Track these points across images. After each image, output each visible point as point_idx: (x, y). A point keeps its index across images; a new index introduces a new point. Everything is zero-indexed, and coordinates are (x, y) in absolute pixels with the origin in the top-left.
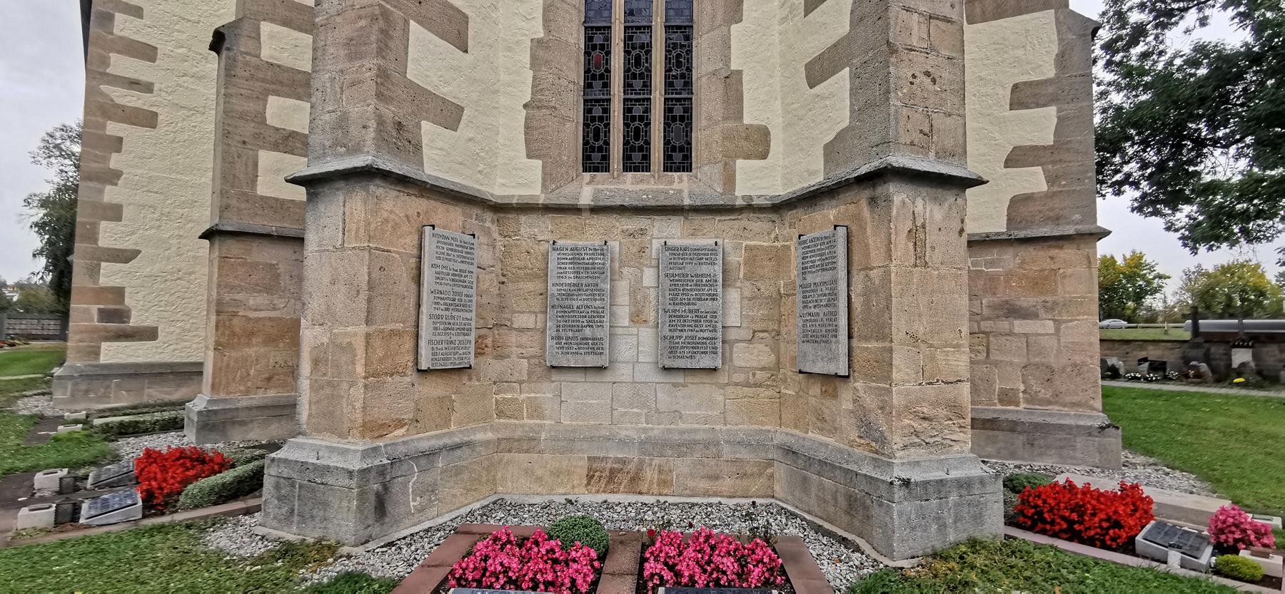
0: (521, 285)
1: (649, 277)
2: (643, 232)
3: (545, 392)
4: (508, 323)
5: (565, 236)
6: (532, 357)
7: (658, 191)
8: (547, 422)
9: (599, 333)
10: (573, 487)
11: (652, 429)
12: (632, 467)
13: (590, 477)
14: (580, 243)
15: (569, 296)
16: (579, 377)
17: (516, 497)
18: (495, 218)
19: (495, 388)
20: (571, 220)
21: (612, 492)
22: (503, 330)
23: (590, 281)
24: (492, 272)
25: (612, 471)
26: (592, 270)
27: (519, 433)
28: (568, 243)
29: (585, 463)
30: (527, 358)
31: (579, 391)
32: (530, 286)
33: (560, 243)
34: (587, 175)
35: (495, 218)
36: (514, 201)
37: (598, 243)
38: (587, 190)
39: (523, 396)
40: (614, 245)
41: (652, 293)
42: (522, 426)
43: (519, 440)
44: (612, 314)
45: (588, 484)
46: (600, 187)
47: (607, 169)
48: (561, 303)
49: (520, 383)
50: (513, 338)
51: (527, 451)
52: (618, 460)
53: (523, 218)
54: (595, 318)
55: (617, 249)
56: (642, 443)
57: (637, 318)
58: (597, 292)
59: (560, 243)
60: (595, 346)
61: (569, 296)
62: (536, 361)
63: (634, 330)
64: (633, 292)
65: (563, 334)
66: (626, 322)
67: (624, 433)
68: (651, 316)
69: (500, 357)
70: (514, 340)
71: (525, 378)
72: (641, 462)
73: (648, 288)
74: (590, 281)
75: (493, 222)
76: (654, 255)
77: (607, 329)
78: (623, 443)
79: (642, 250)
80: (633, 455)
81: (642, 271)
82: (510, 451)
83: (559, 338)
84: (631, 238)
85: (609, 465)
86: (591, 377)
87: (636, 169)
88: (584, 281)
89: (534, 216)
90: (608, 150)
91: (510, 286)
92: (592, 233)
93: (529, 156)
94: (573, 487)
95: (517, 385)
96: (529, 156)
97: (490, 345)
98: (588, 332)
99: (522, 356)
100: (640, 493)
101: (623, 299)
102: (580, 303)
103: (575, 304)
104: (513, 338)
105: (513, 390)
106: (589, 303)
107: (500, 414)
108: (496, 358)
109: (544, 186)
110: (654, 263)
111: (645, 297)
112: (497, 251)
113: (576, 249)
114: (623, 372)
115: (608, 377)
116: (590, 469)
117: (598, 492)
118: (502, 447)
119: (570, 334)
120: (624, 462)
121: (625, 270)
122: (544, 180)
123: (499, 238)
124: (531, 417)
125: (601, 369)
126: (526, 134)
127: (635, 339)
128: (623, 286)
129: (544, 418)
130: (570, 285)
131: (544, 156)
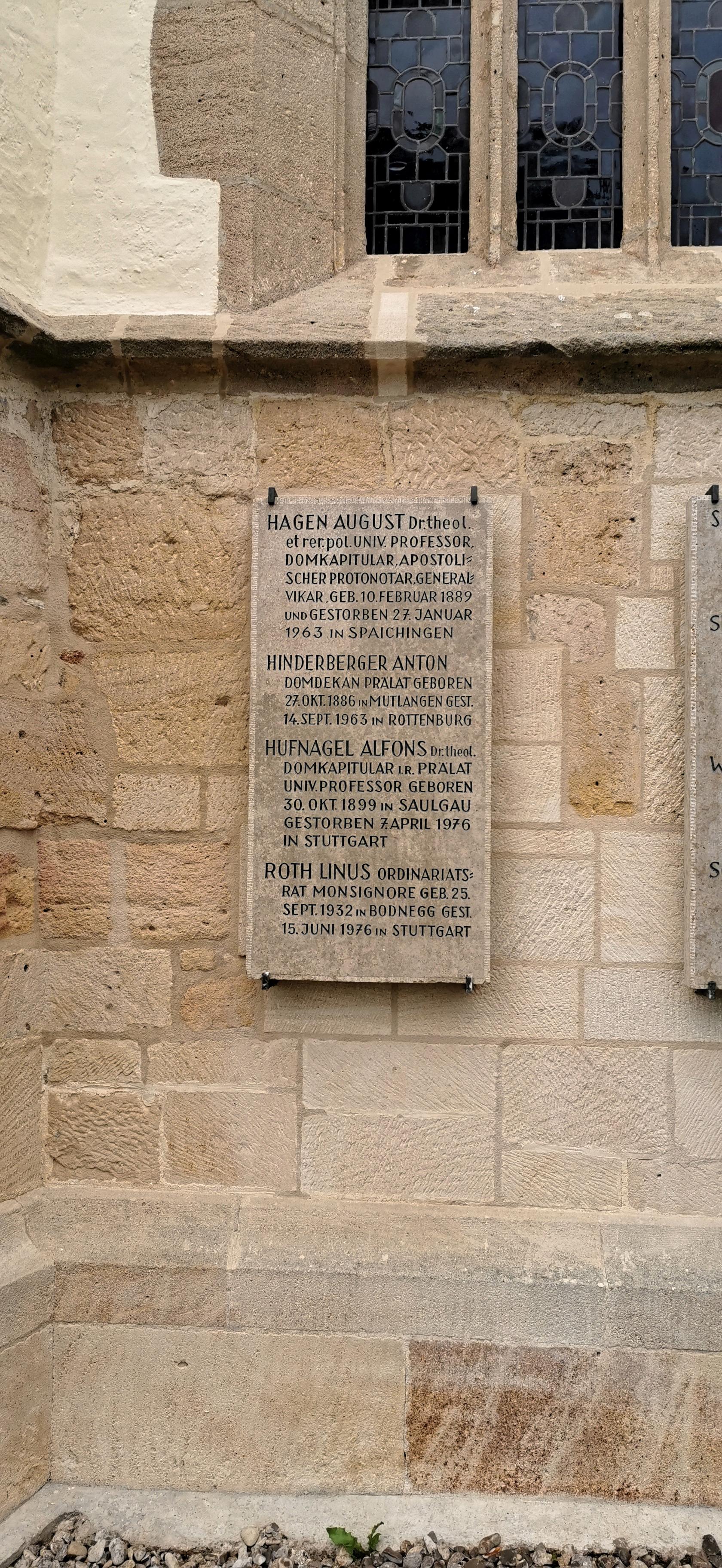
0: (145, 664)
1: (641, 635)
2: (614, 458)
3: (242, 1076)
4: (98, 812)
5: (313, 478)
6: (190, 940)
7: (668, 298)
8: (249, 1195)
9: (449, 849)
10: (355, 1466)
11: (661, 1230)
12: (590, 1389)
13: (422, 1427)
14: (376, 503)
15: (334, 704)
16: (371, 1020)
17: (127, 1505)
18: (44, 406)
19: (48, 1057)
20: (330, 417)
21: (512, 1487)
22: (74, 838)
23: (415, 646)
24: (34, 615)
25: (510, 1405)
26: (415, 600)
27: (136, 1243)
28: (328, 500)
29: (400, 1371)
30: (173, 945)
31: (378, 1088)
32: (180, 668)
33: (291, 502)
34: (386, 264)
35: (44, 406)
36: (117, 333)
37: (444, 500)
38: (394, 304)
39: (156, 1090)
40: (505, 509)
41: (656, 700)
42: (152, 1209)
43: (139, 1272)
44: (499, 780)
45: (415, 1452)
46: (442, 291)
47: (458, 242)
48: (302, 732)
49: (143, 1036)
50: (114, 870)
51: (173, 1318)
52: (533, 1361)
53: (150, 409)
54: (436, 792)
55: (514, 526)
56: (626, 1292)
57: (593, 791)
58: (435, 687)
59: (291, 502)
60: (434, 900)
61: (334, 704)
62: (204, 955)
63: (581, 839)
64: (582, 688)
65: (309, 855)
66: (548, 806)
67: (546, 1249)
68: (653, 784)
69: (74, 938)
70: (118, 875)
71: (163, 1019)
72: (629, 1370)
73: (637, 675)
74: (415, 646)
75: (34, 419)
76: (659, 549)
77: (481, 833)
78: (553, 1292)
79: (611, 530)
80: (593, 1338)
81: (611, 610)
82: (103, 1316)
83: (296, 869)
84: (569, 485)
85: (498, 1380)
86: (415, 1021)
87: (568, 239)
88: (393, 648)
89: (193, 399)
90: (460, 168)
91: (105, 670)
92: (411, 465)
93: (171, 165)
94: (355, 1466)
95: (129, 1049)
96: (171, 165)
97: (27, 893)
98: (407, 846)
99: (147, 936)
100: (625, 1494)
101: (541, 720)
102: (377, 733)
103: (357, 735)
104: (114, 870)
105: (118, 1066)
106: (409, 733)
107: (68, 1157)
108: (49, 943)
109: (229, 280)
110: (660, 577)
111: (627, 712)
112: (55, 538)
113: (361, 521)
114: (542, 1001)
115: (485, 1023)
116: (420, 1393)
117: (453, 1485)
118: (69, 1300)
119: (339, 855)
120: (555, 1366)
121: (547, 609)
122: (228, 257)
123: (59, 484)
124: (185, 1171)
125: (456, 992)
126: (158, 79)
127: (586, 873)
128: (539, 669)
129: (225, 1171)
130: (333, 661)
131: (229, 162)
